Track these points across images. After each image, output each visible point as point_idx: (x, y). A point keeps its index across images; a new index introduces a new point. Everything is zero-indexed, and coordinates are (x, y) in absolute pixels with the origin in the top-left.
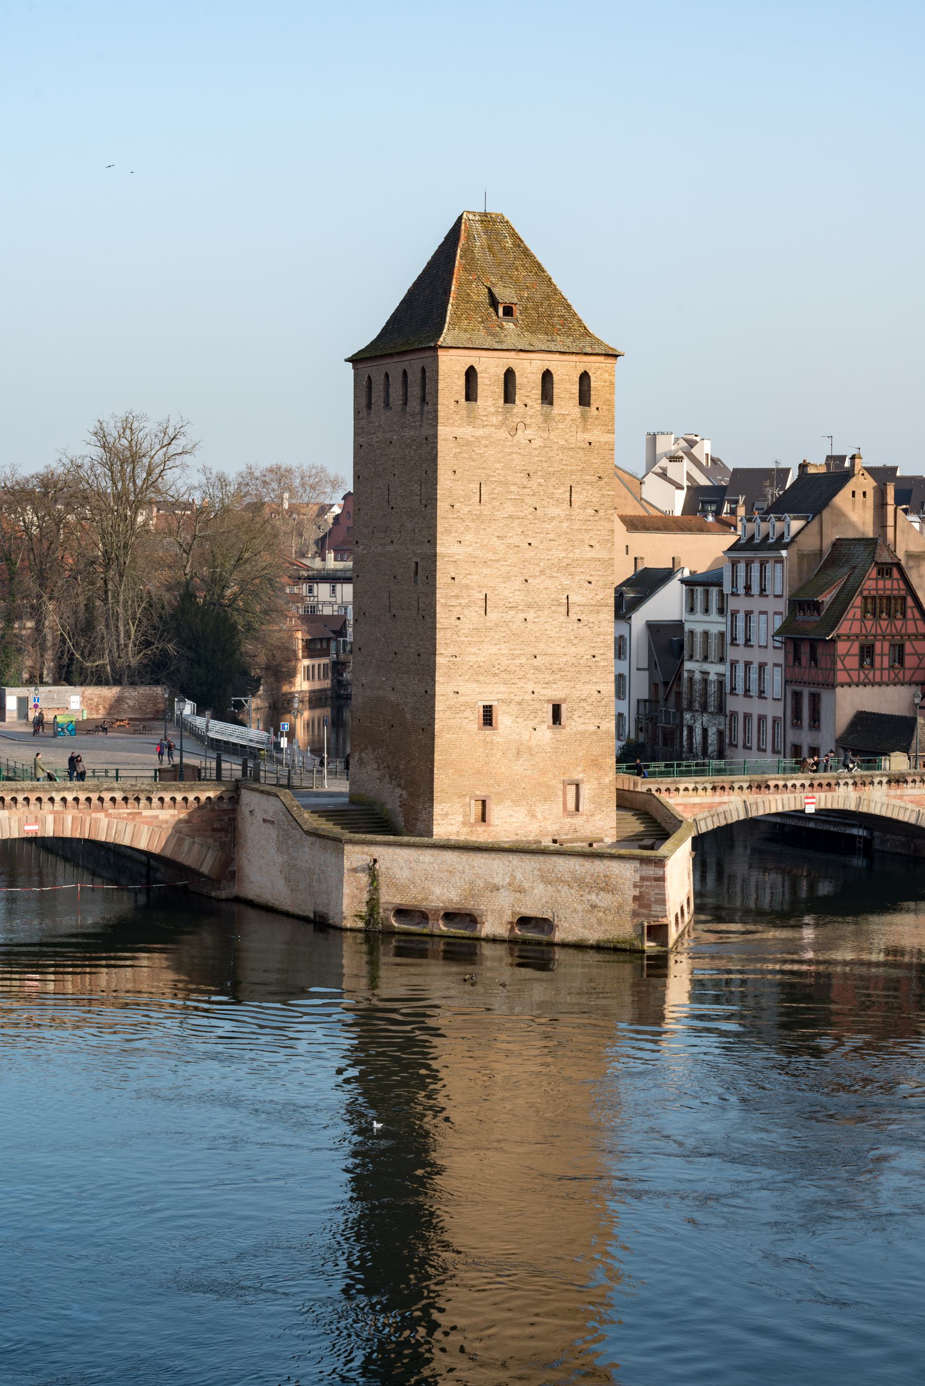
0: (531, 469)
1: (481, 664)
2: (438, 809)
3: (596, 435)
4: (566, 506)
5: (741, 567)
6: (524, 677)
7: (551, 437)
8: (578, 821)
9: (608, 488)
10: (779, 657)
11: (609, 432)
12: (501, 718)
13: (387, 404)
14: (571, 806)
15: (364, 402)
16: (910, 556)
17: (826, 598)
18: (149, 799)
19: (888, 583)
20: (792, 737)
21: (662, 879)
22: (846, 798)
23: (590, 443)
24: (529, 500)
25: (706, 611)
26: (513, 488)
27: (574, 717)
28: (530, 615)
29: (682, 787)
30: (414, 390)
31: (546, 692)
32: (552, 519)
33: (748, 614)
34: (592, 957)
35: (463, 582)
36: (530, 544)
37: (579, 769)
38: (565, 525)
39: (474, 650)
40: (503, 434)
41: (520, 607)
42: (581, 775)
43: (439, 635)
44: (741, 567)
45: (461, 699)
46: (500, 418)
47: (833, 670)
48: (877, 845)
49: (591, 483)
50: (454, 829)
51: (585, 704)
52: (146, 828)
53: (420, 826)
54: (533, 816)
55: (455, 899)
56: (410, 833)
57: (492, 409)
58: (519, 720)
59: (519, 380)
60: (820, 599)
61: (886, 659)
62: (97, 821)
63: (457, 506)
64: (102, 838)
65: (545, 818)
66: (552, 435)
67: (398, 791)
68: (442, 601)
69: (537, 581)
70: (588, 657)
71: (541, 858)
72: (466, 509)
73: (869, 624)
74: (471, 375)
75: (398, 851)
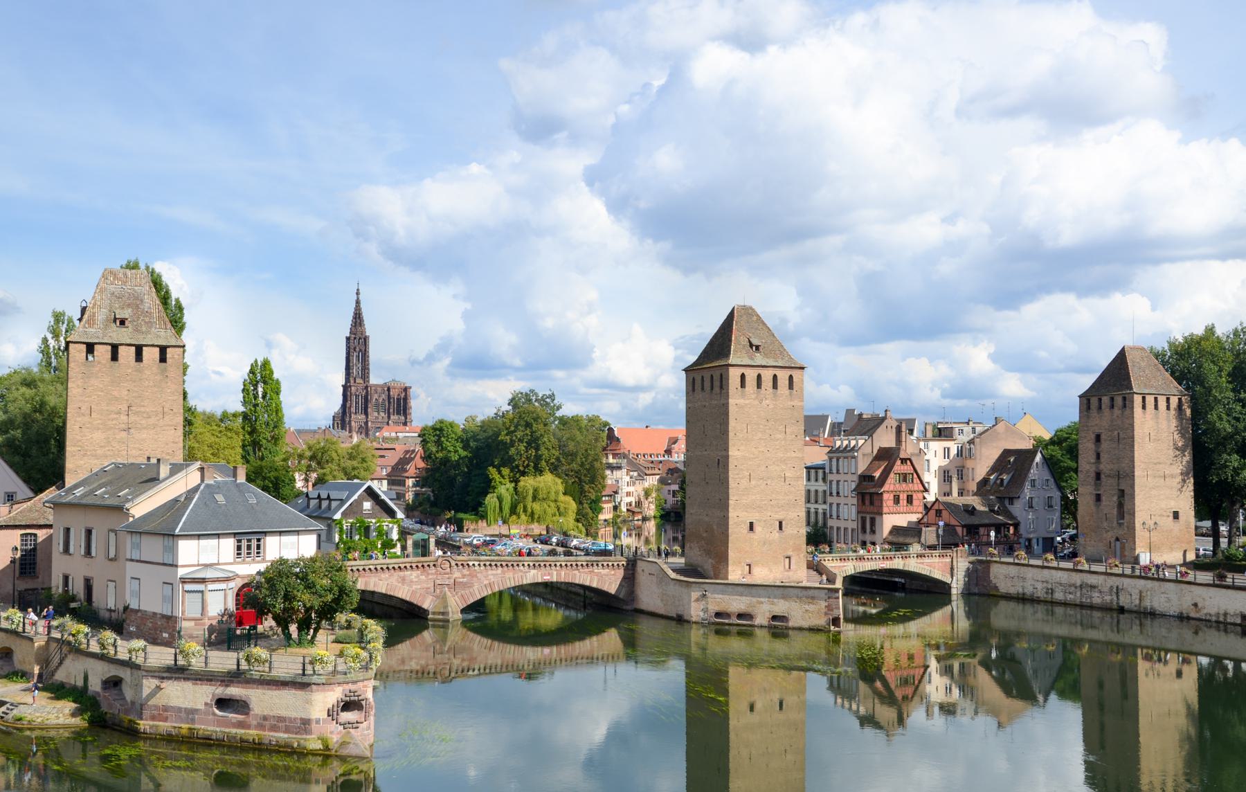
2: (730, 568)
3: (796, 403)
4: (784, 434)
5: (834, 461)
8: (791, 573)
10: (855, 501)
12: (757, 528)
13: (703, 389)
14: (787, 567)
15: (691, 388)
16: (912, 455)
17: (877, 474)
18: (597, 565)
19: (906, 467)
20: (861, 537)
21: (838, 598)
22: (898, 564)
25: (817, 480)
26: (761, 426)
28: (769, 482)
29: (826, 559)
30: (717, 383)
33: (838, 482)
34: (807, 633)
40: (756, 402)
43: (731, 491)
44: (834, 461)
47: (881, 506)
48: (907, 586)
50: (737, 577)
53: (721, 575)
54: (771, 571)
55: (743, 608)
56: (716, 579)
60: (874, 475)
61: (905, 501)
62: (575, 575)
64: (577, 582)
67: (710, 560)
71: (782, 589)
73: (897, 485)
74: (743, 376)
75: (717, 586)
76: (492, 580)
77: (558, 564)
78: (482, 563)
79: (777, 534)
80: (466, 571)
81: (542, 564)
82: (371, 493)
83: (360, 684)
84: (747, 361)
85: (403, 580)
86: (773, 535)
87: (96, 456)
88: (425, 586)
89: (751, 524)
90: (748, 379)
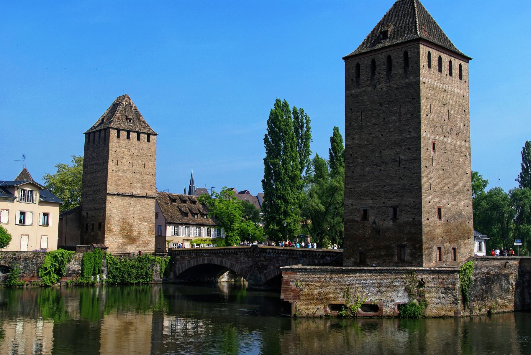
1: (362, 191)
7: (391, 85)
9: (417, 103)
23: (408, 84)
24: (381, 115)
27: (402, 214)
31: (389, 202)
32: (392, 121)
35: (355, 156)
36: (382, 135)
38: (397, 124)
41: (378, 164)
42: (406, 242)
45: (354, 207)
51: (407, 208)
57: (366, 79)
58: (377, 216)
70: (409, 185)
72: (356, 124)
79: (391, 222)
89: (365, 211)
90: (362, 67)
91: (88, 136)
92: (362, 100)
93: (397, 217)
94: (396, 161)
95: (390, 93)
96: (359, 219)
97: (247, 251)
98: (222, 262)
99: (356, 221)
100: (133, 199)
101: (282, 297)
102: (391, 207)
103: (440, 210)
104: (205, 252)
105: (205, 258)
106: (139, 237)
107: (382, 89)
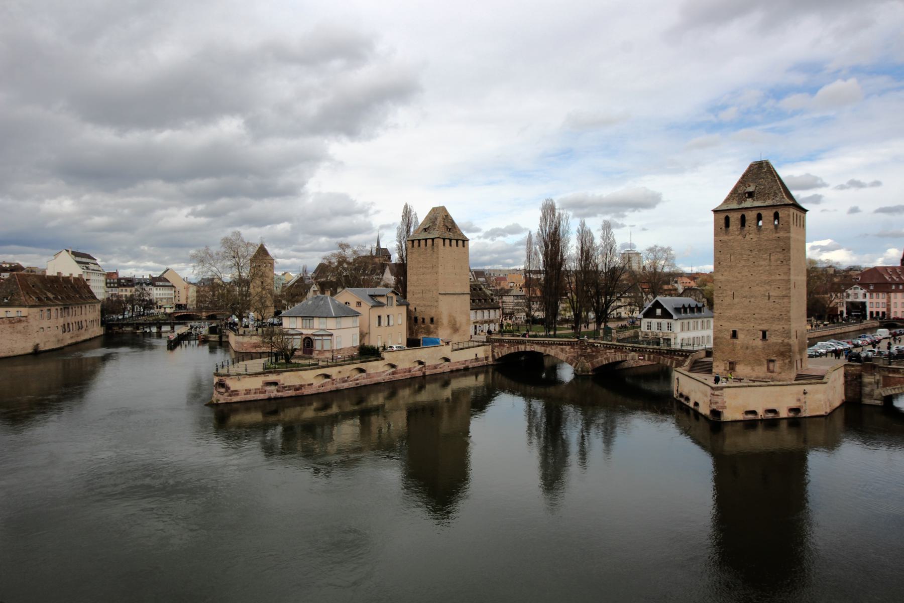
0: (752, 249)
3: (782, 234)
6: (749, 321)
8: (774, 375)
11: (788, 233)
18: (675, 353)
23: (779, 237)
24: (751, 259)
29: (901, 371)
31: (759, 327)
32: (762, 266)
37: (774, 355)
38: (768, 268)
39: (729, 311)
40: (740, 237)
46: (739, 232)
49: (779, 252)
51: (777, 332)
52: (675, 361)
54: (753, 370)
59: (746, 218)
62: (660, 358)
63: (721, 263)
65: (759, 372)
66: (762, 236)
68: (716, 295)
69: (755, 288)
72: (725, 264)
76: (609, 356)
77: (648, 350)
78: (602, 345)
80: (594, 349)
81: (638, 349)
82: (657, 305)
83: (223, 378)
84: (734, 205)
85: (562, 350)
86: (756, 341)
87: (414, 286)
88: (573, 354)
90: (732, 220)
91: (411, 242)
92: (731, 245)
93: (767, 338)
94: (765, 296)
95: (761, 243)
96: (729, 337)
97: (574, 344)
98: (545, 350)
99: (725, 339)
100: (456, 296)
101: (715, 408)
102: (760, 330)
103: (796, 332)
104: (528, 342)
105: (527, 346)
106: (460, 327)
107: (752, 239)
